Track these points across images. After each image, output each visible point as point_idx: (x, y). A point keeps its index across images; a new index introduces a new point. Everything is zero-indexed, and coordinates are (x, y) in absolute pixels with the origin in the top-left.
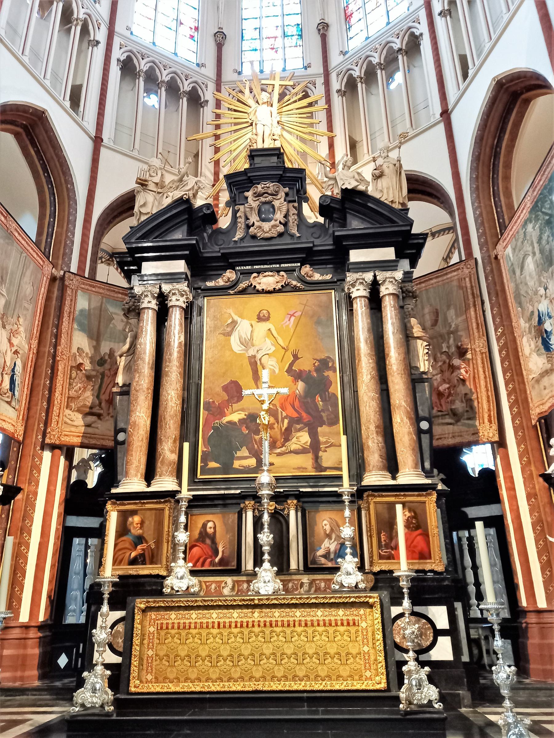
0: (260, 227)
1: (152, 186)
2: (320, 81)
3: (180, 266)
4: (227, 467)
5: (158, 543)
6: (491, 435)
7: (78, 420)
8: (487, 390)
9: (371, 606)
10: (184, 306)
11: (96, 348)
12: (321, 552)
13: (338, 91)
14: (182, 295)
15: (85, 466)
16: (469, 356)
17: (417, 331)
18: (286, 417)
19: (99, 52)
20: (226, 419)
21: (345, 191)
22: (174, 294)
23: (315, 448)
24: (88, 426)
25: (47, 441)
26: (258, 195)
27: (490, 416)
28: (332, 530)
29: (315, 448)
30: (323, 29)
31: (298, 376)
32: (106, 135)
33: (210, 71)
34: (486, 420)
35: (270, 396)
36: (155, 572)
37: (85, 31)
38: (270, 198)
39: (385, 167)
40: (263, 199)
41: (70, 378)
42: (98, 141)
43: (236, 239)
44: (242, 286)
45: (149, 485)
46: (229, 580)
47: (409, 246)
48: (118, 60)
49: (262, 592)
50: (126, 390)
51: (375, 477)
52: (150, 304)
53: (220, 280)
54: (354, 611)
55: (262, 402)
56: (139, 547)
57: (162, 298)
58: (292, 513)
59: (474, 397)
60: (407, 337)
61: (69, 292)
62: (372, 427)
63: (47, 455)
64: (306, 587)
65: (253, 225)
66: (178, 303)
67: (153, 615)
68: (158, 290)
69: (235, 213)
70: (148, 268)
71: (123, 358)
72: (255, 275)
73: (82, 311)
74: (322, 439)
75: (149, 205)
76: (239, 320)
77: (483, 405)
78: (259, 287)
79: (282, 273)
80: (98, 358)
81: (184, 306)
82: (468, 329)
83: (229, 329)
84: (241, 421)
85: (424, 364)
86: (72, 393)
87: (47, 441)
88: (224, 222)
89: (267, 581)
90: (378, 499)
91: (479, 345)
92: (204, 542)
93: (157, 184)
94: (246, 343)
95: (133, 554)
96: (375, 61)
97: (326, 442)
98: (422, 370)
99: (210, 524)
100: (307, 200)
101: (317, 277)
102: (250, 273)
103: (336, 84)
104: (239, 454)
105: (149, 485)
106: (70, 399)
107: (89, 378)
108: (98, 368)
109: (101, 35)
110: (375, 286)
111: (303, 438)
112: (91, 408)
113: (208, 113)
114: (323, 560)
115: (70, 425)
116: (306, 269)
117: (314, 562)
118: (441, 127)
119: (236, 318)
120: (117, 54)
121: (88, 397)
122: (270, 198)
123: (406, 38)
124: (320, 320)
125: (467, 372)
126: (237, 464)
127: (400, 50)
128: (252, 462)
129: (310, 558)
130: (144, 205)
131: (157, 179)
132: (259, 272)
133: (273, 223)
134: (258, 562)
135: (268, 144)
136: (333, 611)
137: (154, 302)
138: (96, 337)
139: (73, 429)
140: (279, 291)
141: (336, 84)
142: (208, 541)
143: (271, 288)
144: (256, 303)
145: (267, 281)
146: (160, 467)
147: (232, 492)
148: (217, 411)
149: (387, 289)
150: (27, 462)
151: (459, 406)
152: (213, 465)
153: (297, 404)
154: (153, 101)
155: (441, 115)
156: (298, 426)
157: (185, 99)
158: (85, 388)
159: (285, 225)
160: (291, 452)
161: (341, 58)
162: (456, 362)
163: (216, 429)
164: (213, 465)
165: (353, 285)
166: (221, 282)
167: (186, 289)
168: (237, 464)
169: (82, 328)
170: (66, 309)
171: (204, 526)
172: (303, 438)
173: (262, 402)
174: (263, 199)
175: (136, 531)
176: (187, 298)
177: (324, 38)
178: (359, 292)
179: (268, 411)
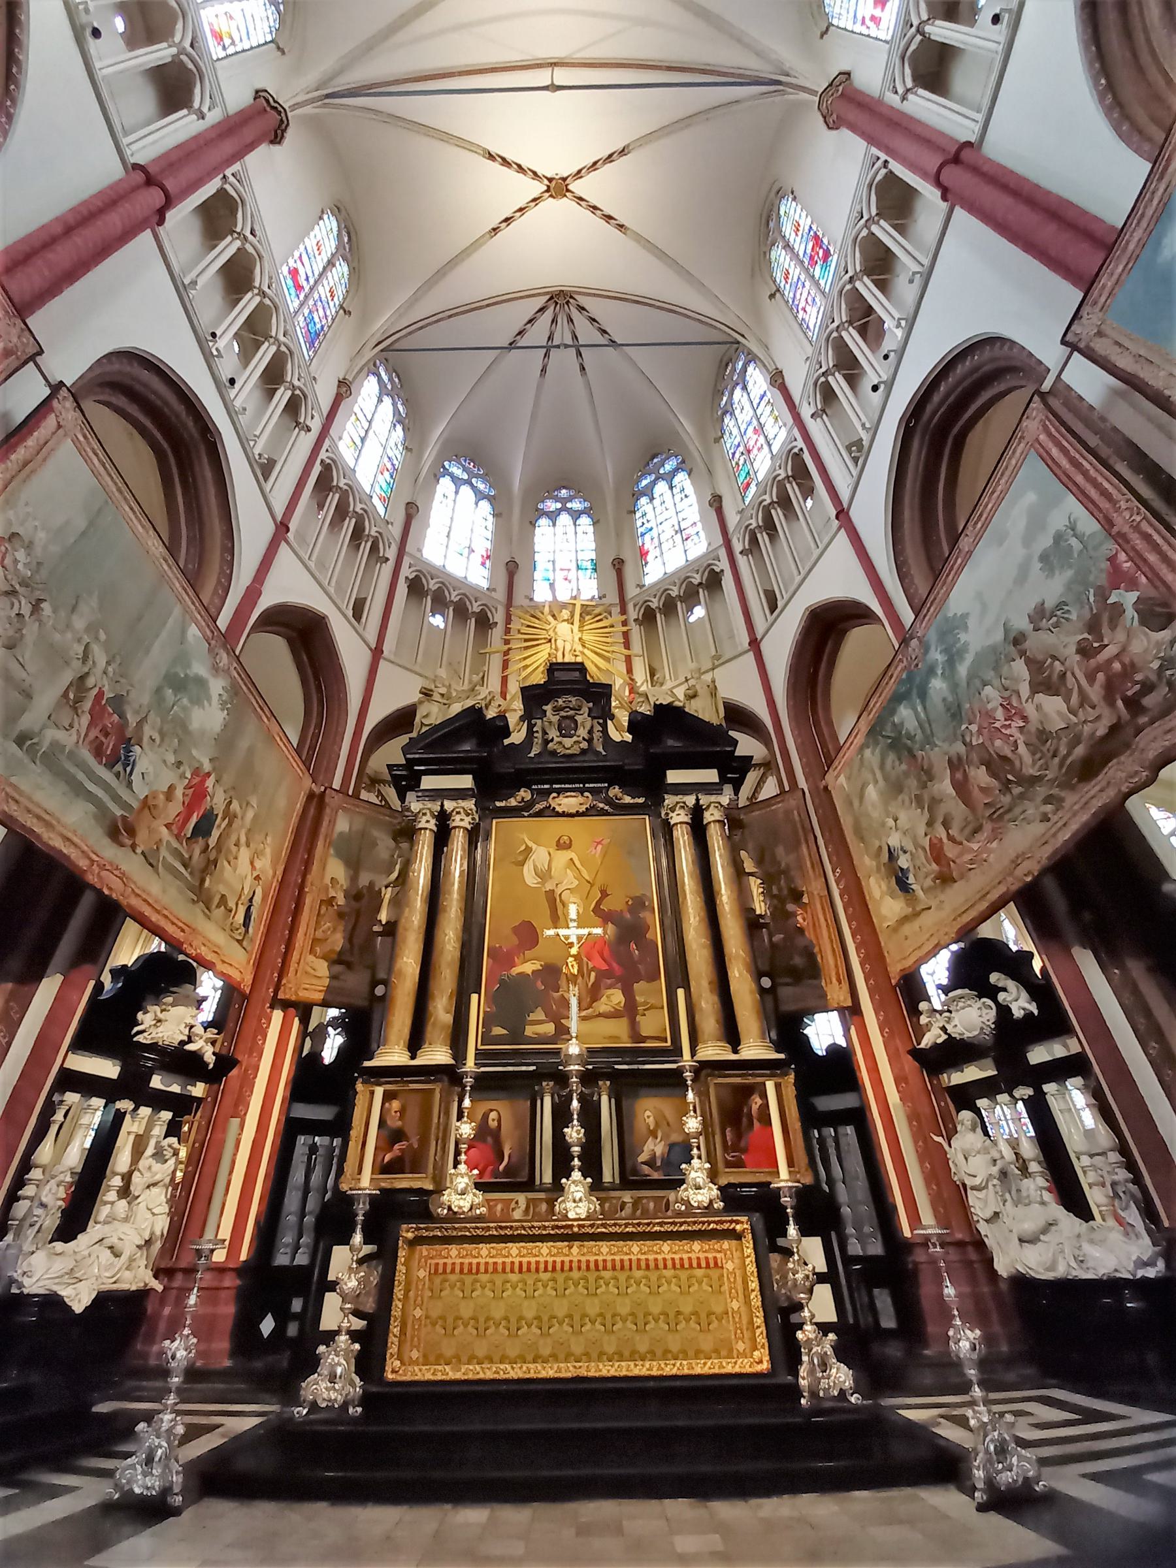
0: (560, 743)
1: (436, 697)
3: (466, 781)
4: (516, 1035)
5: (424, 1141)
6: (842, 998)
7: (322, 968)
8: (832, 941)
9: (738, 1236)
10: (469, 827)
11: (354, 879)
12: (643, 1158)
13: (635, 620)
14: (468, 815)
15: (320, 1035)
16: (805, 900)
17: (749, 866)
18: (593, 969)
19: (387, 569)
20: (515, 971)
21: (658, 708)
22: (458, 813)
23: (630, 1010)
24: (333, 977)
25: (281, 996)
26: (557, 710)
27: (838, 974)
28: (657, 1124)
29: (630, 1010)
30: (618, 565)
31: (605, 917)
32: (387, 648)
33: (500, 595)
34: (834, 980)
35: (579, 938)
36: (417, 1185)
37: (374, 548)
38: (572, 712)
39: (698, 687)
40: (563, 713)
41: (319, 914)
42: (377, 653)
43: (532, 755)
44: (538, 807)
45: (413, 1057)
46: (521, 1198)
47: (734, 770)
48: (407, 578)
49: (571, 1215)
50: (391, 930)
52: (428, 823)
53: (512, 800)
54: (714, 1244)
55: (571, 945)
56: (397, 1147)
57: (443, 818)
58: (604, 1099)
59: (816, 950)
60: (739, 873)
61: (328, 811)
62: (705, 984)
63: (278, 1016)
64: (628, 1209)
65: (552, 740)
66: (462, 824)
67: (424, 1250)
68: (439, 808)
69: (531, 727)
70: (428, 782)
71: (390, 889)
72: (555, 795)
73: (341, 834)
74: (639, 999)
75: (433, 715)
76: (534, 847)
77: (828, 960)
78: (558, 809)
79: (586, 794)
80: (354, 893)
81: (469, 827)
82: (801, 867)
83: (521, 858)
84: (533, 972)
85: (760, 907)
86: (319, 934)
87: (281, 996)
88: (517, 737)
89: (577, 1201)
90: (720, 1080)
91: (816, 887)
92: (484, 1141)
93: (442, 695)
94: (544, 875)
95: (387, 1158)
96: (674, 594)
97: (646, 1003)
98: (758, 912)
99: (493, 1115)
100: (612, 717)
101: (628, 800)
102: (548, 793)
103: (633, 614)
104: (532, 1017)
105: (413, 1057)
106: (315, 941)
107: (341, 915)
108: (353, 903)
109: (391, 553)
110: (697, 812)
111: (615, 998)
112: (340, 953)
113: (497, 634)
114: (646, 1169)
115: (311, 975)
116: (615, 791)
117: (635, 1171)
118: (750, 656)
119: (530, 844)
120: (406, 572)
121: (338, 941)
122: (572, 712)
123: (706, 573)
125: (804, 920)
126: (530, 1031)
127: (700, 584)
128: (549, 1028)
129: (629, 1164)
130: (426, 716)
131: (443, 690)
132: (559, 792)
133: (575, 739)
134: (562, 1168)
135: (569, 659)
136: (685, 1245)
137: (433, 821)
138: (354, 865)
139: (314, 981)
140: (583, 814)
142: (489, 1139)
143: (573, 811)
145: (569, 802)
146: (431, 1032)
147: (524, 1068)
148: (504, 959)
149: (711, 816)
150: (250, 1025)
151: (798, 961)
152: (498, 1031)
153: (606, 953)
154: (438, 621)
155: (750, 644)
156: (609, 981)
157: (473, 620)
158: (335, 929)
159: (590, 741)
160: (600, 1015)
161: (638, 590)
162: (791, 907)
163: (502, 983)
164: (498, 1031)
165: (673, 810)
166: (513, 802)
167: (473, 807)
168: (530, 1031)
169: (339, 855)
170: (323, 830)
171: (486, 1116)
172: (615, 998)
173: (571, 945)
174: (563, 713)
176: (473, 819)
178: (679, 817)
179: (577, 957)
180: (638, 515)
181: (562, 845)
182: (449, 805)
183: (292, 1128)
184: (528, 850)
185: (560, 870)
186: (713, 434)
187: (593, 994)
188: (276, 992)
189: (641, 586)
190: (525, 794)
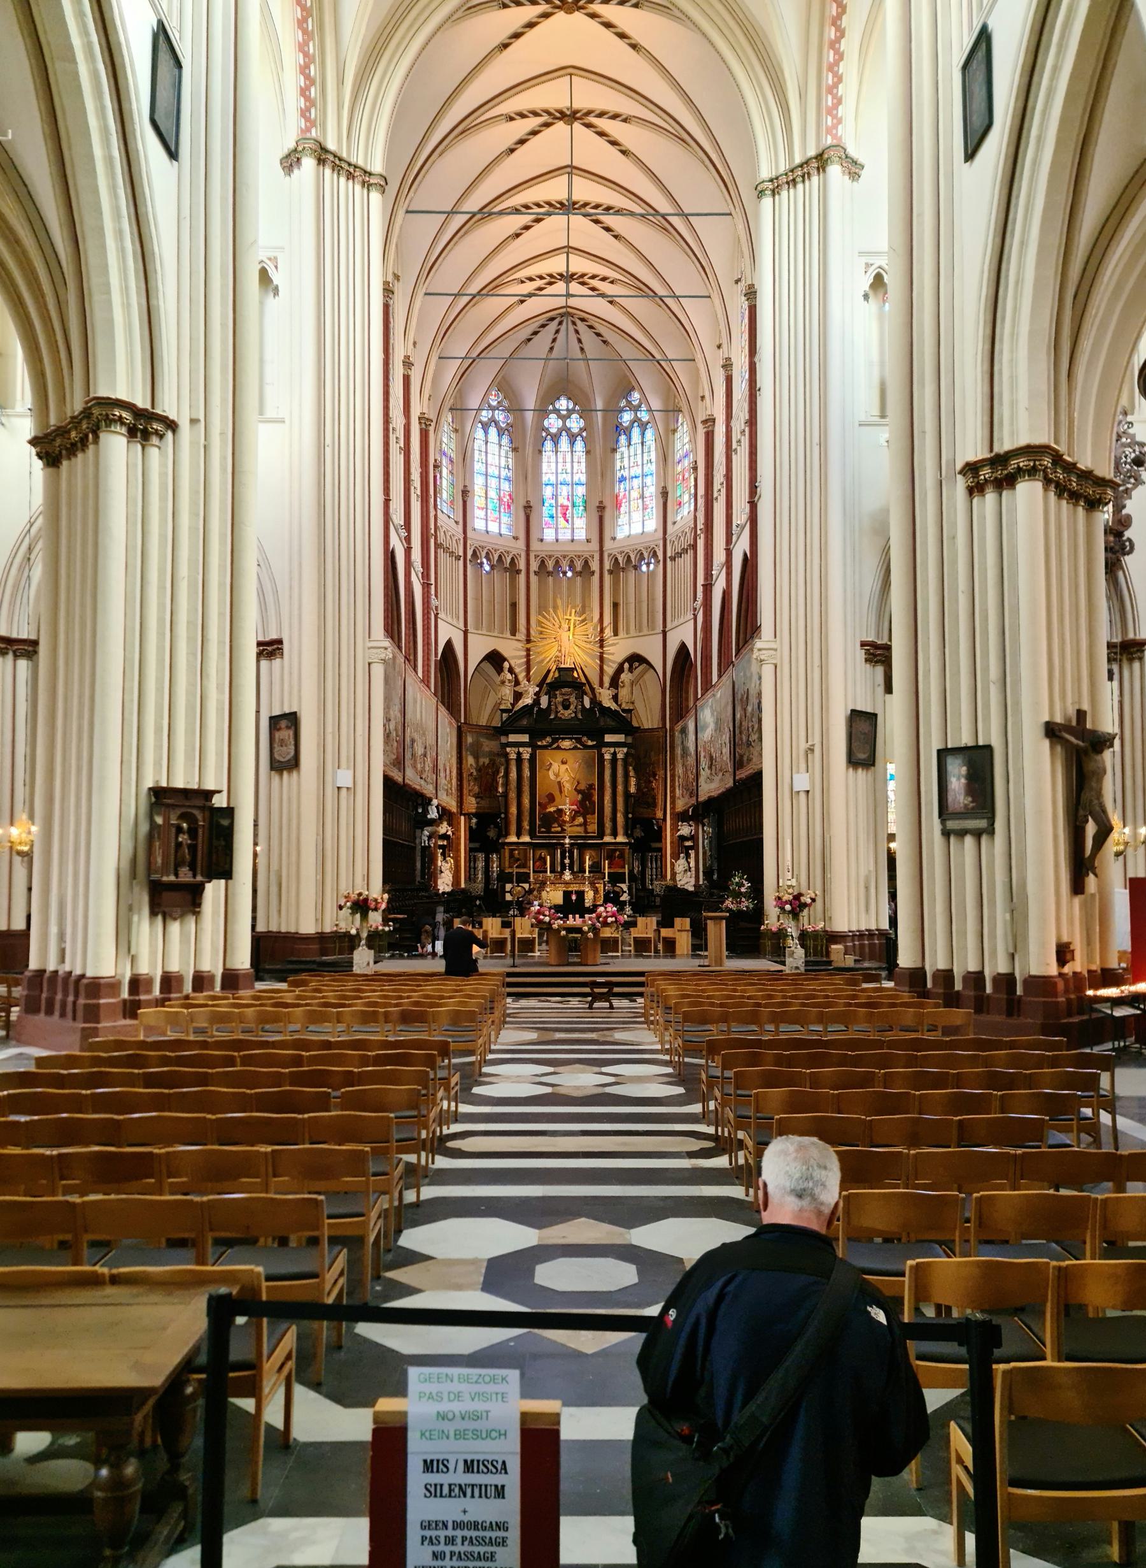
2: (597, 557)
4: (549, 831)
11: (477, 762)
17: (632, 774)
23: (585, 824)
29: (585, 824)
30: (601, 508)
31: (579, 792)
42: (466, 633)
50: (505, 795)
51: (608, 839)
85: (633, 790)
101: (590, 743)
103: (607, 565)
110: (614, 754)
111: (581, 820)
113: (522, 577)
115: (471, 804)
116: (585, 739)
120: (470, 553)
124: (588, 764)
132: (563, 739)
134: (563, 868)
138: (476, 758)
141: (607, 565)
144: (560, 755)
148: (543, 806)
149: (620, 756)
150: (455, 822)
151: (650, 800)
172: (581, 820)
175: (517, 856)
177: (601, 519)
180: (618, 456)
181: (563, 763)
182: (521, 749)
183: (471, 850)
185: (563, 769)
186: (672, 427)
187: (573, 819)
188: (461, 809)
189: (614, 539)
190: (549, 739)
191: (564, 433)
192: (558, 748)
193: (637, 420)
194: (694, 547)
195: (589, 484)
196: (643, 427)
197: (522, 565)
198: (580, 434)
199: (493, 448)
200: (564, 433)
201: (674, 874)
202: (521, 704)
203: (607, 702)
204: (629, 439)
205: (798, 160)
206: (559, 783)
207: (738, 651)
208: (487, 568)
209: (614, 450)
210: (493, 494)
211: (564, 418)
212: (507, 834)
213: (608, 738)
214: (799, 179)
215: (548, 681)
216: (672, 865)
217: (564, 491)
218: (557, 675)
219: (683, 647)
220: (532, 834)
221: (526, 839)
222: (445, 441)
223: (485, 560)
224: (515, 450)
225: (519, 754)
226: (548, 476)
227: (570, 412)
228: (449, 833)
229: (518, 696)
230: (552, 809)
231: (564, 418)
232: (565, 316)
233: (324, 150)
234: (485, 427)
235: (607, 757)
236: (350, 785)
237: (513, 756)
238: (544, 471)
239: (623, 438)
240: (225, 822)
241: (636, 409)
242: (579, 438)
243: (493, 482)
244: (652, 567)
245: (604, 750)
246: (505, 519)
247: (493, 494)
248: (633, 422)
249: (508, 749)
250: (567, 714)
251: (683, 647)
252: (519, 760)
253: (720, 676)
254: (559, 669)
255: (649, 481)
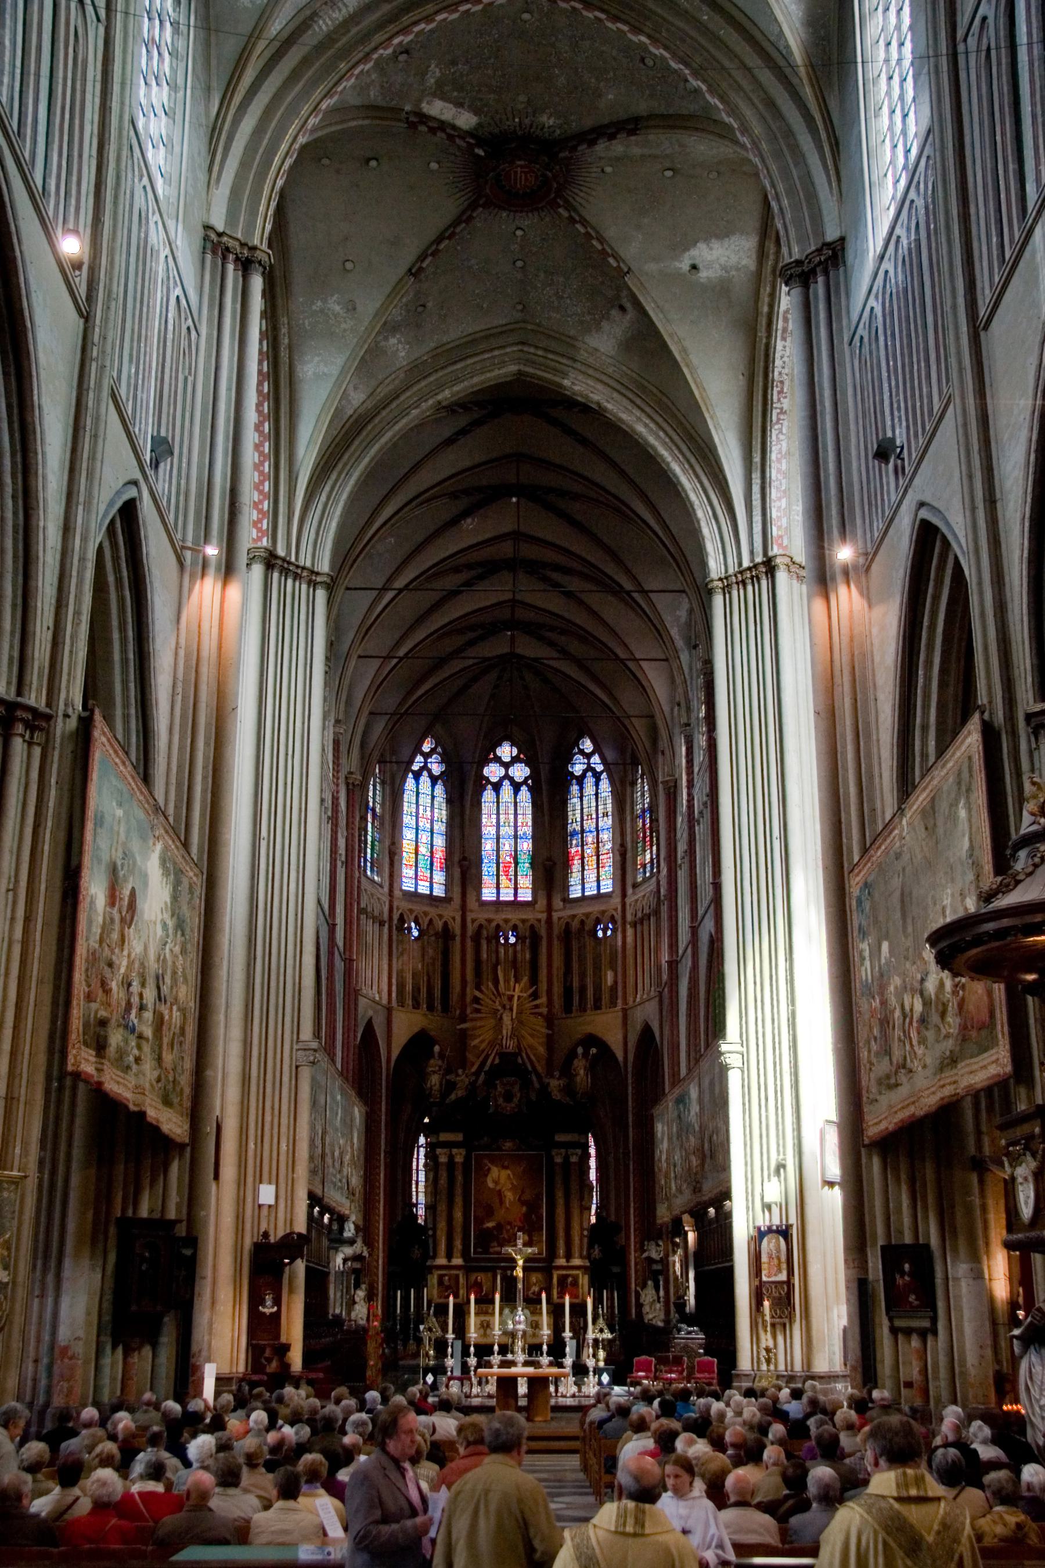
31: (523, 1203)
110: (566, 1158)
120: (396, 917)
148: (479, 1221)
175: (446, 1283)
178: (558, 1160)
182: (455, 1151)
184: (489, 1169)
189: (567, 900)
191: (506, 783)
192: (500, 1149)
193: (589, 768)
194: (657, 912)
195: (536, 838)
196: (597, 776)
197: (458, 931)
198: (525, 782)
199: (425, 800)
200: (506, 783)
201: (639, 1306)
202: (453, 1097)
203: (557, 1095)
204: (581, 789)
205: (746, 563)
206: (500, 1194)
207: (707, 1046)
208: (416, 933)
209: (564, 802)
210: (423, 850)
211: (506, 766)
212: (434, 1257)
213: (560, 1138)
214: (749, 581)
215: (486, 1068)
216: (638, 1295)
217: (507, 846)
218: (497, 1061)
219: (647, 1030)
220: (465, 1254)
221: (458, 1261)
222: (374, 795)
223: (413, 925)
224: (449, 801)
225: (451, 1157)
226: (488, 829)
227: (515, 760)
228: (366, 1254)
229: (451, 1086)
230: (490, 1225)
231: (506, 766)
232: (511, 661)
233: (276, 557)
234: (417, 775)
235: (558, 1160)
236: (272, 1202)
237: (443, 1159)
238: (484, 821)
239: (575, 788)
240: (188, 1252)
241: (588, 756)
242: (524, 788)
243: (424, 837)
244: (609, 933)
245: (554, 1152)
246: (439, 877)
247: (423, 850)
248: (585, 772)
249: (439, 1151)
250: (509, 1107)
251: (647, 1030)
252: (451, 1164)
253: (689, 1070)
254: (502, 1055)
255: (605, 836)
